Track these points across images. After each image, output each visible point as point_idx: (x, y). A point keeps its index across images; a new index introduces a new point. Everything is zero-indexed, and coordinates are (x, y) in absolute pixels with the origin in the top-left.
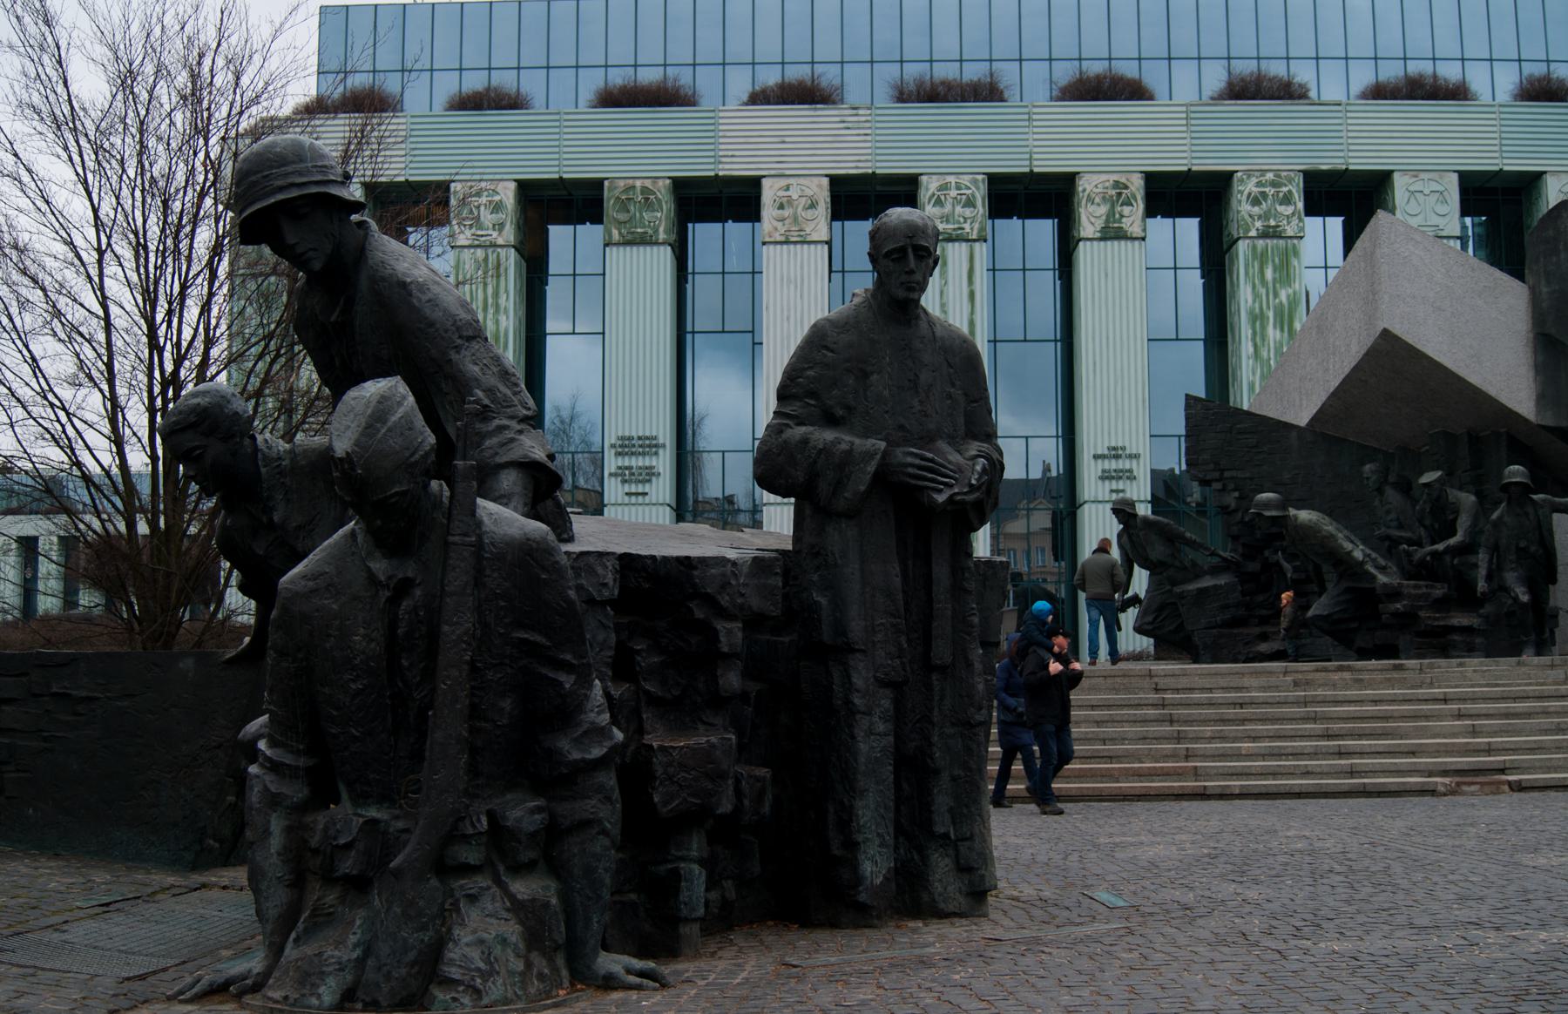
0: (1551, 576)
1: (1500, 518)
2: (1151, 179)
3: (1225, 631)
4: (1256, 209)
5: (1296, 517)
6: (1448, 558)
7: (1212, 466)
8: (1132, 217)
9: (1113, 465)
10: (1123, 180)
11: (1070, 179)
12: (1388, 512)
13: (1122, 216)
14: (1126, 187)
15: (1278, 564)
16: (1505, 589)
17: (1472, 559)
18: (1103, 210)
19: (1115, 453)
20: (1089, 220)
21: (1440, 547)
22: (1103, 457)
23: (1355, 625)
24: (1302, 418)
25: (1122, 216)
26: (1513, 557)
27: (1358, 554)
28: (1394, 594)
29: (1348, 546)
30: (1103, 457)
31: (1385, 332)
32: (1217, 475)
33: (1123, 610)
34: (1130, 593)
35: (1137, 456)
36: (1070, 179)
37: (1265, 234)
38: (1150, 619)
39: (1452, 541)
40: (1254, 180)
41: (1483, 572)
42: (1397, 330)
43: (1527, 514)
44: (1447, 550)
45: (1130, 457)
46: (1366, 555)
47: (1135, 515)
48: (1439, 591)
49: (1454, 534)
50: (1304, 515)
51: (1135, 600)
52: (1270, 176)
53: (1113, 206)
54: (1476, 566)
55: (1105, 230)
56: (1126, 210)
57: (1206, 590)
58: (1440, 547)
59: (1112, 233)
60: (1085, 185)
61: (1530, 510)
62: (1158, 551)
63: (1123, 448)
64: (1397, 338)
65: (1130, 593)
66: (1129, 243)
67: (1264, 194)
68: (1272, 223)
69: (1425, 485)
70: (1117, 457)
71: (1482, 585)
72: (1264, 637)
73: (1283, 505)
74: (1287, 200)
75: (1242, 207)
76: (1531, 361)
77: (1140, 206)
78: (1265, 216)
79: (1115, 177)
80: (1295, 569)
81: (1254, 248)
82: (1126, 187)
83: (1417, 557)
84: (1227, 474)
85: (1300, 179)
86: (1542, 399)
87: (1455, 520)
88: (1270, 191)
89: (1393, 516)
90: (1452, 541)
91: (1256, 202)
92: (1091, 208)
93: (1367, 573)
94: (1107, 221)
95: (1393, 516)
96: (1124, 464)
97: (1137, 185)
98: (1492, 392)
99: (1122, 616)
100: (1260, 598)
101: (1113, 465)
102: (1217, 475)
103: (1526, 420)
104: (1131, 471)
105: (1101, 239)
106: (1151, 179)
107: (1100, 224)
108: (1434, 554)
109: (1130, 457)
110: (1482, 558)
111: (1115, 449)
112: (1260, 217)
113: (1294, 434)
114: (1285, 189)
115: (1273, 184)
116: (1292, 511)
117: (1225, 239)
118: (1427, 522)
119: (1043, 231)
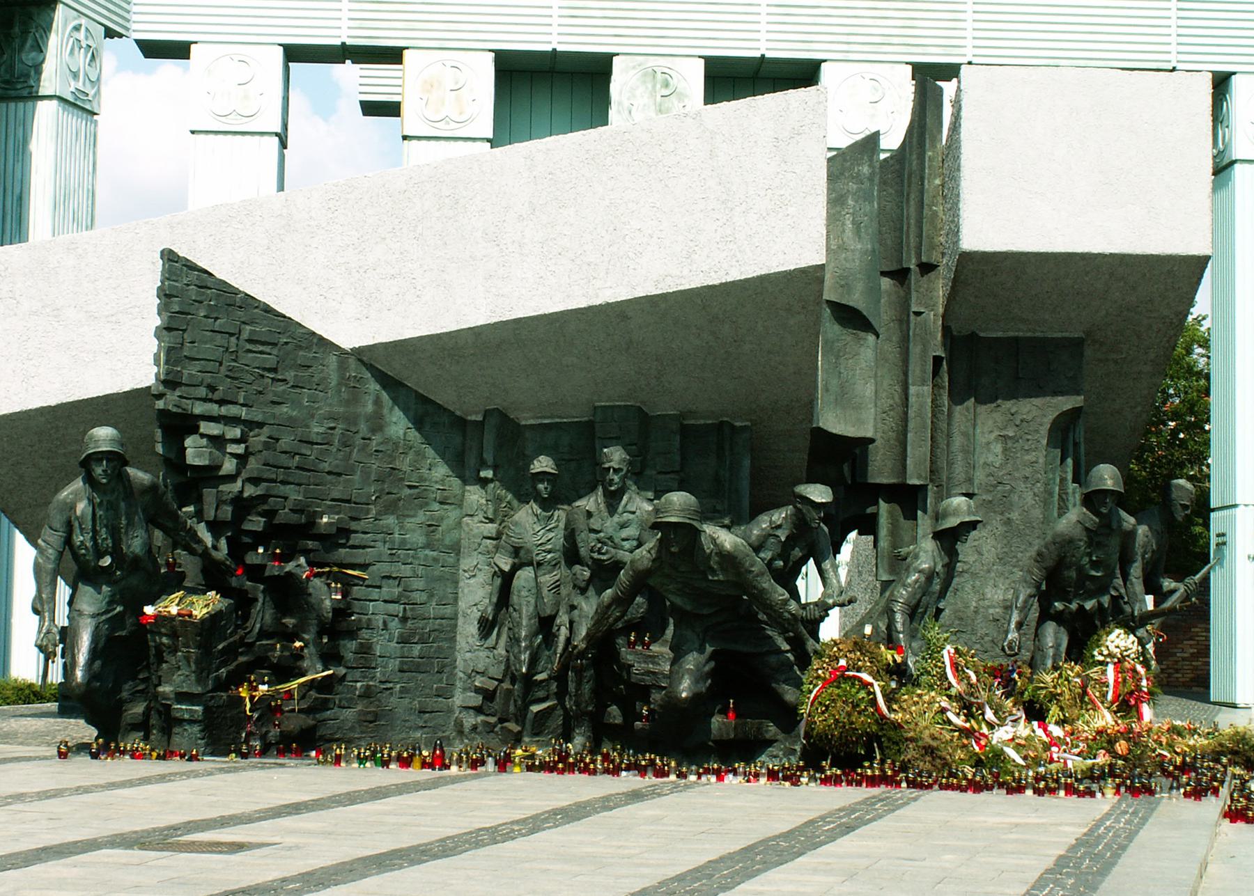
12: (623, 526)
89: (625, 533)
113: (332, 360)
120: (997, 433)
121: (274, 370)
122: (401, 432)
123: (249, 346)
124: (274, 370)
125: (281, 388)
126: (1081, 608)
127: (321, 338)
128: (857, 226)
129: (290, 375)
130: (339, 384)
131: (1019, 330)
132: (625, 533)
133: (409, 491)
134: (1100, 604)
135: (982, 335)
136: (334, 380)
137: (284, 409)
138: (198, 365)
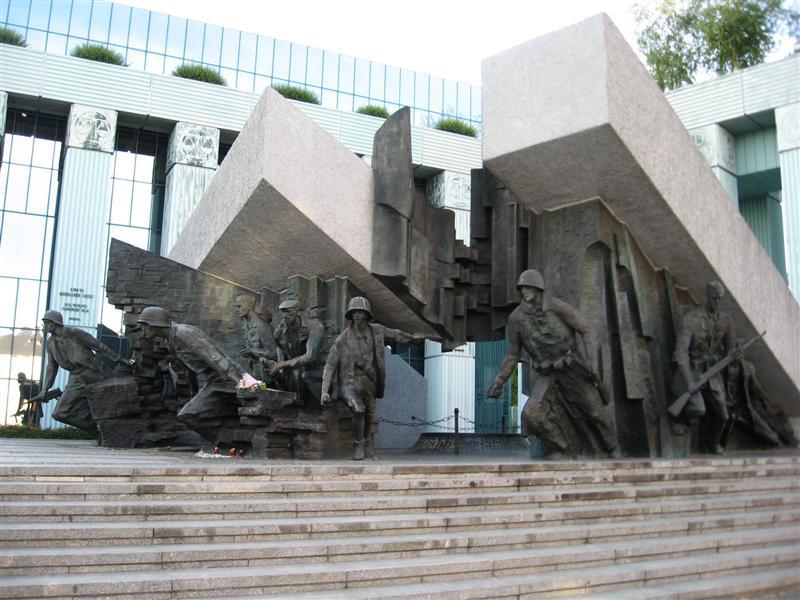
0: (379, 394)
1: (345, 339)
2: (122, 117)
3: (122, 422)
4: (188, 146)
5: (176, 328)
6: (296, 373)
7: (125, 294)
8: (108, 139)
9: (74, 301)
10: (103, 112)
11: (66, 107)
12: (252, 335)
13: (99, 136)
14: (104, 119)
15: (168, 372)
16: (342, 400)
17: (316, 373)
18: (87, 130)
19: (76, 293)
20: (76, 133)
21: (292, 362)
22: (67, 294)
23: (217, 424)
24: (196, 265)
25: (99, 136)
26: (352, 374)
27: (224, 364)
28: (251, 398)
29: (215, 356)
30: (67, 294)
31: (265, 188)
32: (128, 300)
33: (46, 400)
34: (55, 387)
35: (91, 297)
36: (66, 107)
37: (191, 164)
38: (66, 409)
39: (303, 358)
40: (189, 129)
41: (325, 385)
42: (272, 182)
43: (365, 338)
44: (298, 366)
45: (86, 296)
46: (230, 365)
47: (62, 326)
48: (291, 398)
49: (304, 352)
50: (182, 328)
51: (57, 393)
52: (199, 128)
53: (94, 129)
54: (321, 380)
55: (87, 143)
56: (102, 133)
57: (112, 387)
58: (292, 362)
59: (91, 146)
60: (75, 112)
61: (368, 334)
62: (77, 355)
63: (82, 290)
64: (272, 189)
65: (55, 387)
66: (102, 154)
67: (194, 139)
68: (197, 157)
69: (284, 310)
70: (76, 295)
71: (325, 395)
72: (152, 428)
73: (168, 318)
74: (209, 144)
75: (179, 146)
76: (370, 225)
77: (112, 132)
78: (193, 153)
79: (99, 111)
80: (180, 377)
81: (184, 171)
82: (104, 119)
83: (273, 370)
84: (136, 301)
85: (218, 133)
86: (376, 253)
87: (305, 342)
88: (198, 137)
89: (255, 338)
90: (303, 358)
91: (189, 143)
92: (79, 128)
93: (229, 380)
94: (89, 138)
95: (255, 338)
96: (78, 301)
97: (112, 120)
98: (341, 242)
99: (44, 405)
100: (153, 397)
101: (74, 301)
102: (128, 300)
103: (364, 270)
104: (85, 306)
105: (85, 148)
106: (122, 117)
107: (84, 138)
108: (288, 369)
109: (86, 296)
110: (327, 373)
111: (76, 290)
112: (190, 153)
113: (189, 274)
114: (208, 138)
115: (201, 134)
116: (174, 324)
117: (167, 164)
118: (283, 342)
119: (48, 148)
120: (557, 266)
121: (160, 282)
122: (225, 304)
123: (148, 273)
124: (160, 282)
125: (163, 289)
126: (552, 366)
127: (184, 267)
128: (389, 160)
129: (167, 283)
130: (192, 285)
131: (565, 203)
132: (254, 339)
133: (229, 331)
134: (565, 363)
135: (550, 210)
136: (189, 284)
137: (165, 298)
138: (125, 283)
